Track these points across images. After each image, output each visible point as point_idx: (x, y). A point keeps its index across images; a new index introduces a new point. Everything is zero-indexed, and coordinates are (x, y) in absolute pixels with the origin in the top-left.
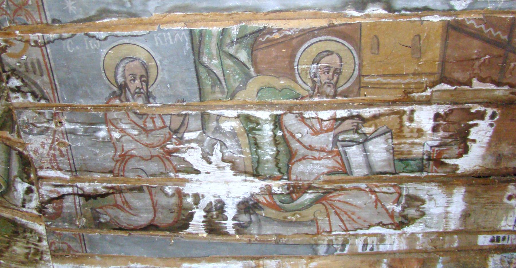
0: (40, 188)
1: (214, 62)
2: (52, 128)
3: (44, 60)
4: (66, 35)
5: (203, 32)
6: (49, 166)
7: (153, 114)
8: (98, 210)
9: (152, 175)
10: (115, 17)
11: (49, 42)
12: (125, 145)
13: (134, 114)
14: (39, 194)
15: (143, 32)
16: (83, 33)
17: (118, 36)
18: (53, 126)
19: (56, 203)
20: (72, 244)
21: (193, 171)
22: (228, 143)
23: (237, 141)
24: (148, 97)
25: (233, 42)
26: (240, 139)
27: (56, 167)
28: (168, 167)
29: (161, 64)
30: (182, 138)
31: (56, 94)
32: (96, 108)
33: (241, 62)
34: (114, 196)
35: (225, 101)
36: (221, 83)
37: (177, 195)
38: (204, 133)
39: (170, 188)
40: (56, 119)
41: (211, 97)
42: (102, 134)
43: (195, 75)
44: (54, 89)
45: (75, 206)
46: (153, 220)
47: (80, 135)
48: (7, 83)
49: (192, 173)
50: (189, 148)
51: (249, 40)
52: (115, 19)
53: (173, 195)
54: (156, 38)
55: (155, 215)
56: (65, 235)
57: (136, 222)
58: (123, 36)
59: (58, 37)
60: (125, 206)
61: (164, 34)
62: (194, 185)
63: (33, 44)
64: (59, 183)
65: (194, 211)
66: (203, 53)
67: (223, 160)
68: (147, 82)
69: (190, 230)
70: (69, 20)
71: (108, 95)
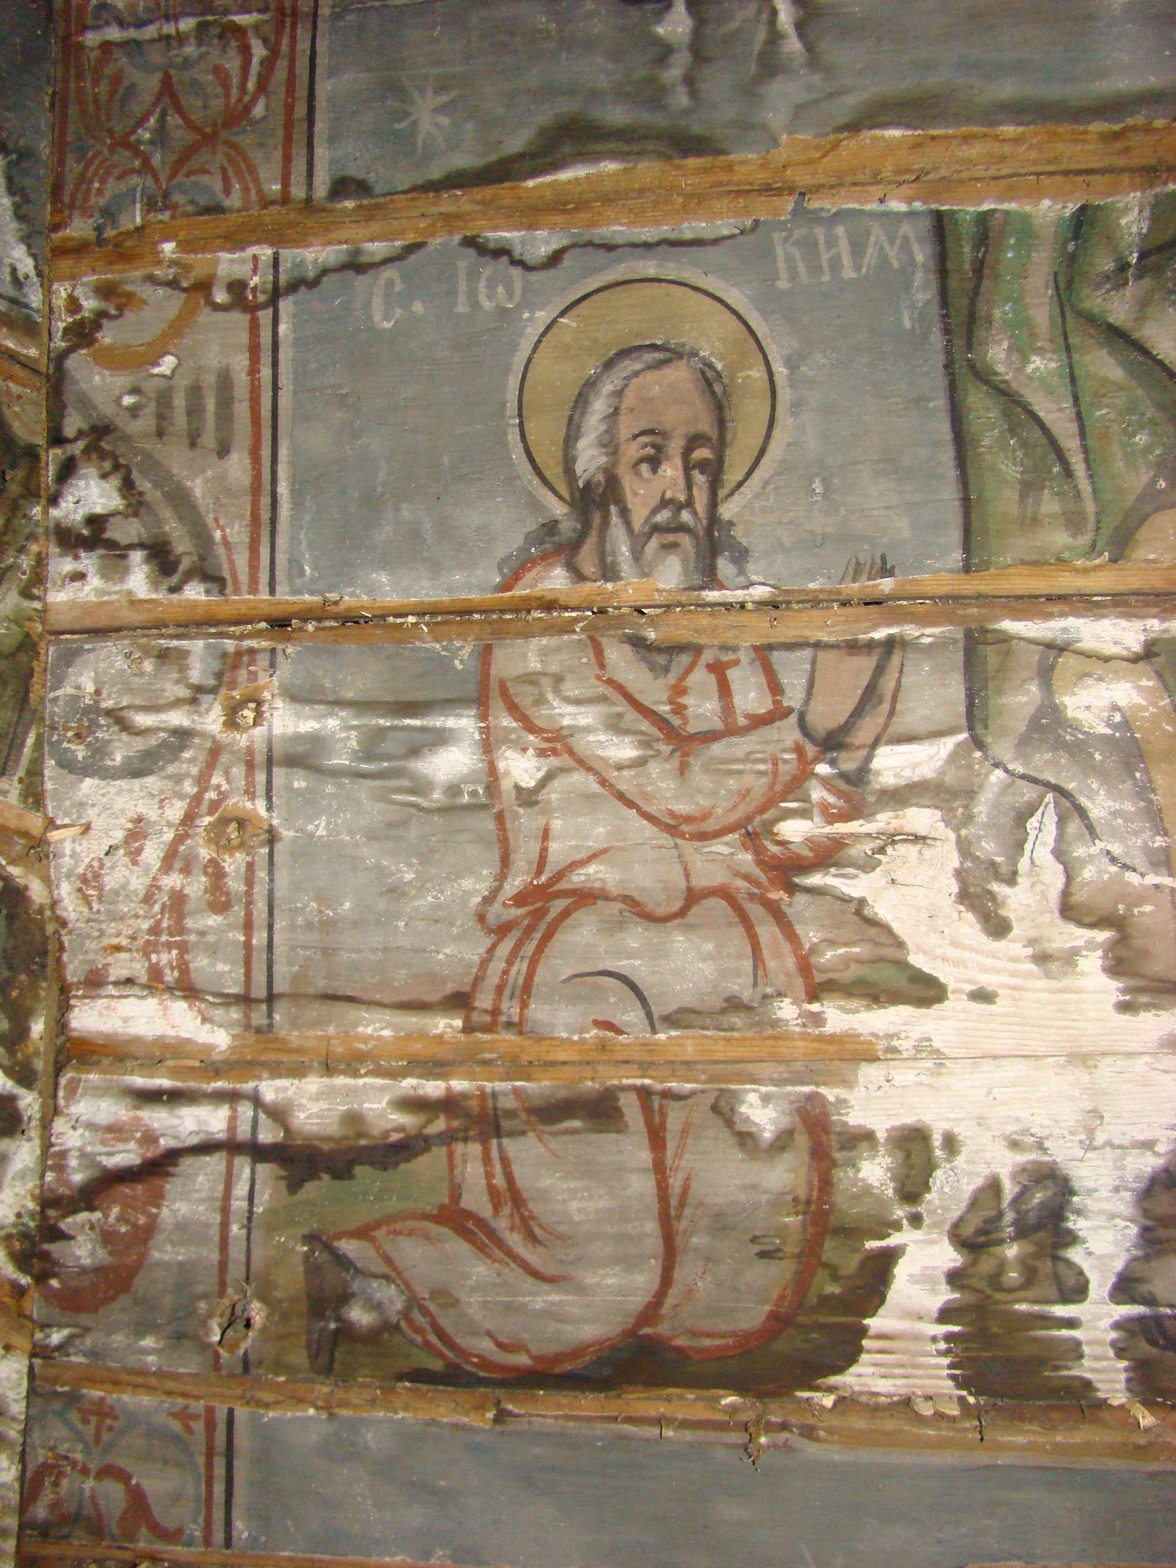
0: (56, 1112)
1: (1037, 362)
2: (203, 735)
3: (253, 371)
5: (994, 224)
6: (139, 969)
7: (725, 648)
8: (348, 1247)
9: (672, 1020)
10: (614, 155)
11: (293, 287)
12: (557, 824)
13: (627, 648)
14: (46, 1145)
16: (457, 238)
17: (610, 248)
18: (212, 721)
19: (125, 1206)
20: (157, 1484)
21: (900, 981)
22: (1099, 806)
23: (1144, 791)
24: (713, 546)
25: (1123, 267)
26: (1160, 780)
27: (170, 976)
28: (771, 964)
29: (792, 381)
30: (859, 777)
31: (265, 552)
32: (450, 616)
33: (1160, 363)
34: (451, 1156)
35: (1086, 571)
36: (1068, 473)
37: (802, 1141)
38: (978, 743)
39: (766, 1099)
40: (233, 685)
41: (1021, 545)
42: (451, 763)
43: (944, 430)
44: (264, 525)
45: (225, 1225)
46: (651, 1312)
47: (336, 773)
48: (54, 500)
49: (896, 998)
50: (891, 838)
52: (611, 166)
53: (783, 1141)
54: (780, 252)
55: (666, 1280)
56: (133, 1420)
57: (553, 1327)
58: (635, 246)
59: (343, 259)
60: (500, 1226)
62: (904, 1075)
63: (220, 297)
64: (165, 1083)
65: (894, 1240)
66: (989, 320)
67: (1069, 910)
68: (715, 471)
69: (866, 1376)
71: (519, 540)
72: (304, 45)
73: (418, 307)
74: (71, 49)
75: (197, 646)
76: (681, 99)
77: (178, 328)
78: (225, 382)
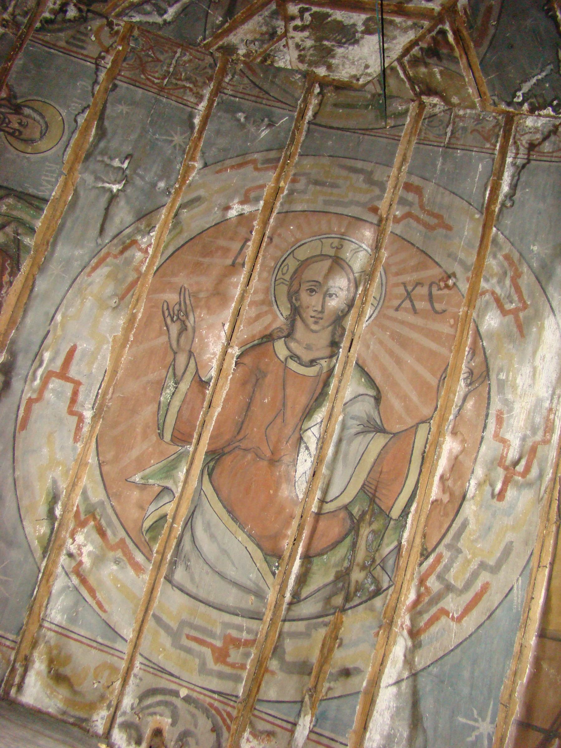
1: (5, 208)
3: (82, 54)
4: (97, 88)
11: (97, 69)
15: (66, 157)
25: (18, 234)
31: (40, 42)
44: (46, 44)
51: (13, 250)
52: (91, 139)
61: (55, 175)
63: (103, 54)
66: (19, 202)
70: (110, 99)
71: (16, 90)
72: (153, 90)
73: (79, 91)
74: (179, 46)
75: (26, 21)
76: (99, 158)
77: (100, 43)
78: (83, 48)
